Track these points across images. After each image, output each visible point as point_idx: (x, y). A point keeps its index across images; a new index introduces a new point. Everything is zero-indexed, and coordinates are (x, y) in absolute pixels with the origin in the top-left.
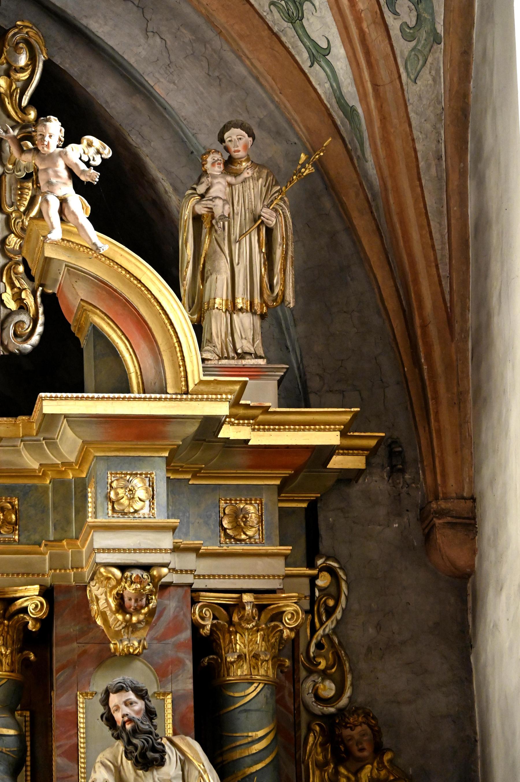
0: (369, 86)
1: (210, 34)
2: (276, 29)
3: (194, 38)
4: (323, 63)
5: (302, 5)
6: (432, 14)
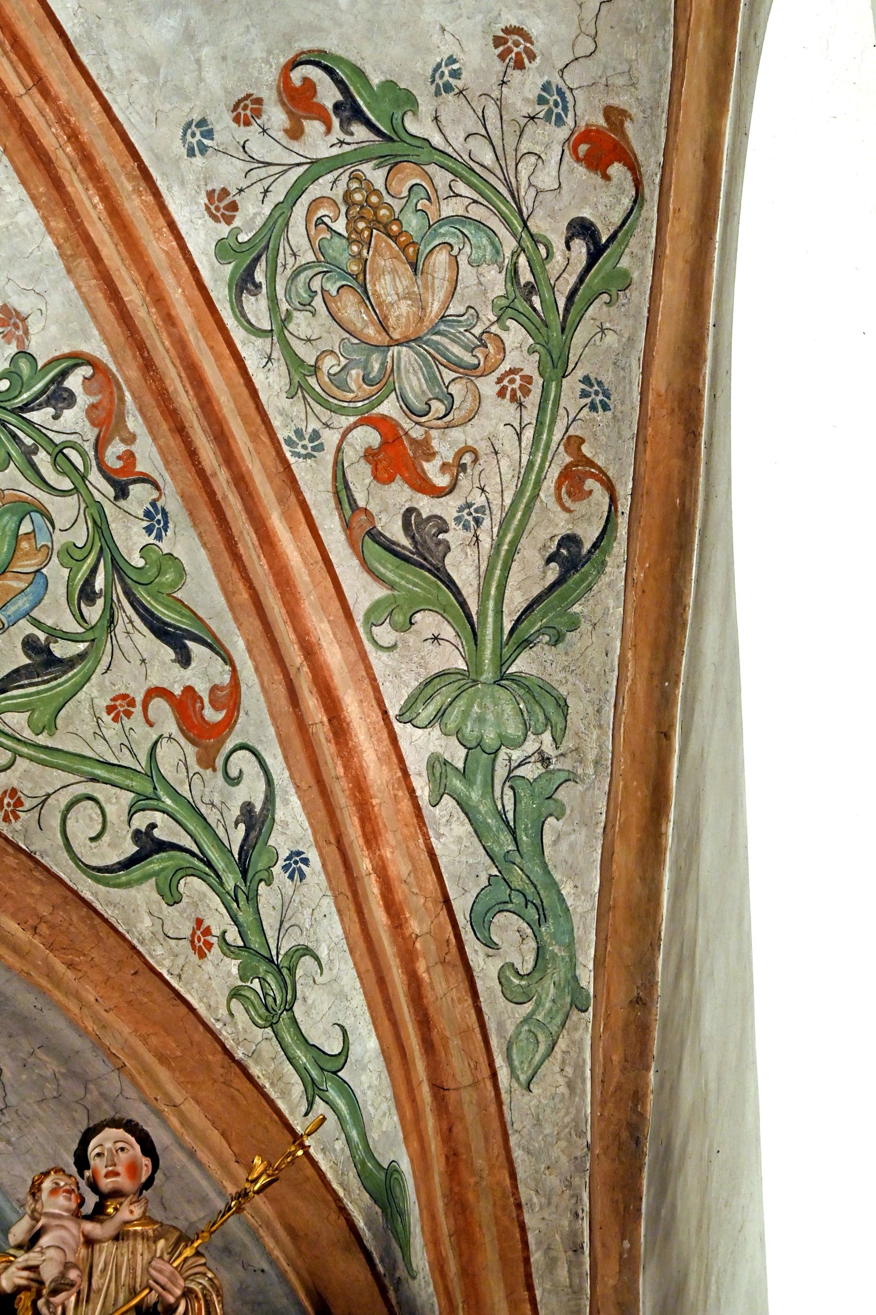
0: (425, 1092)
1: (98, 1066)
2: (239, 1054)
3: (63, 1070)
4: (332, 1094)
5: (292, 970)
6: (570, 947)
